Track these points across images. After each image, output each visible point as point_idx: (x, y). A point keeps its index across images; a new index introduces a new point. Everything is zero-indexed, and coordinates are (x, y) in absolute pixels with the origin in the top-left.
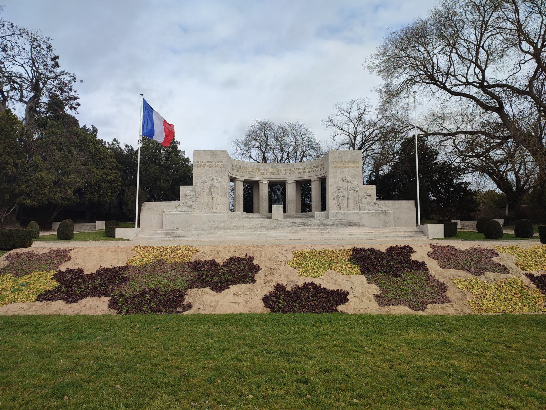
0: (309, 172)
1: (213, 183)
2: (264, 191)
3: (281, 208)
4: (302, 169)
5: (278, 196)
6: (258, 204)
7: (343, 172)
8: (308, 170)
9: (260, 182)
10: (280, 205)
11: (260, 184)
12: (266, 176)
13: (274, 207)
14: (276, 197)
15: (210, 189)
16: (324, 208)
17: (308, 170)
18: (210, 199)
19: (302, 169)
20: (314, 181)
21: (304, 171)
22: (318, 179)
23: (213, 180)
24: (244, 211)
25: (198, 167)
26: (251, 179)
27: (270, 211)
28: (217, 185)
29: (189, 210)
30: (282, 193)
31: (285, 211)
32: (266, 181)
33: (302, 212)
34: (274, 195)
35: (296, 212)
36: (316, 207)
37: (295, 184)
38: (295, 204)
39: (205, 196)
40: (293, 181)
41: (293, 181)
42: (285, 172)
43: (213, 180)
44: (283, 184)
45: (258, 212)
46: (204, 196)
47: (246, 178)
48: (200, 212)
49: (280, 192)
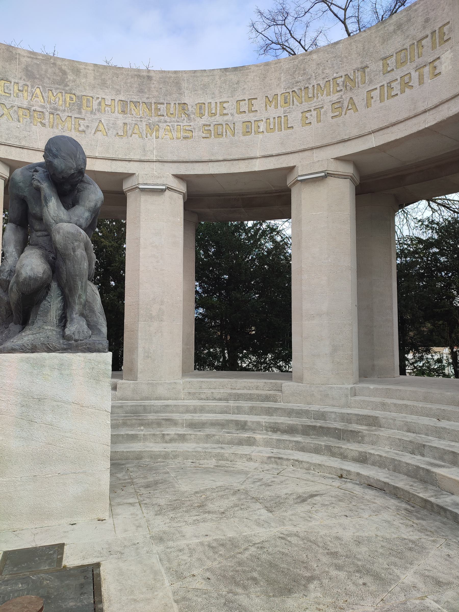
4: (230, 107)
8: (273, 112)
17: (273, 112)
19: (230, 107)
20: (328, 175)
21: (251, 117)
22: (349, 170)
35: (185, 373)
36: (335, 349)
42: (121, 119)
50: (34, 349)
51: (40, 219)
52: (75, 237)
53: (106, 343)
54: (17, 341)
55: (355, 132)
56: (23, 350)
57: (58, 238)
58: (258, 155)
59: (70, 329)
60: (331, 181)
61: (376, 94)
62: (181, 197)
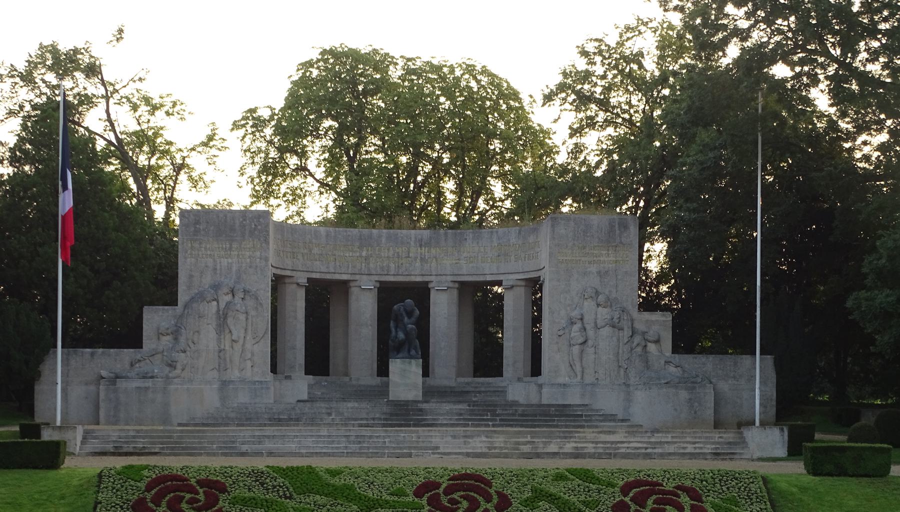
3: (415, 368)
5: (407, 334)
6: (346, 346)
9: (352, 284)
10: (411, 357)
11: (354, 291)
13: (395, 365)
16: (536, 370)
20: (512, 287)
22: (523, 283)
24: (306, 374)
26: (328, 277)
30: (417, 323)
31: (426, 373)
32: (369, 283)
34: (396, 327)
35: (459, 374)
37: (455, 293)
39: (213, 334)
40: (451, 285)
41: (451, 285)
47: (314, 276)
49: (413, 319)
50: (403, 358)
51: (402, 320)
52: (412, 329)
53: (420, 356)
54: (398, 356)
55: (521, 271)
56: (401, 358)
57: (408, 329)
58: (488, 273)
59: (411, 353)
60: (514, 288)
61: (527, 256)
62: (456, 290)
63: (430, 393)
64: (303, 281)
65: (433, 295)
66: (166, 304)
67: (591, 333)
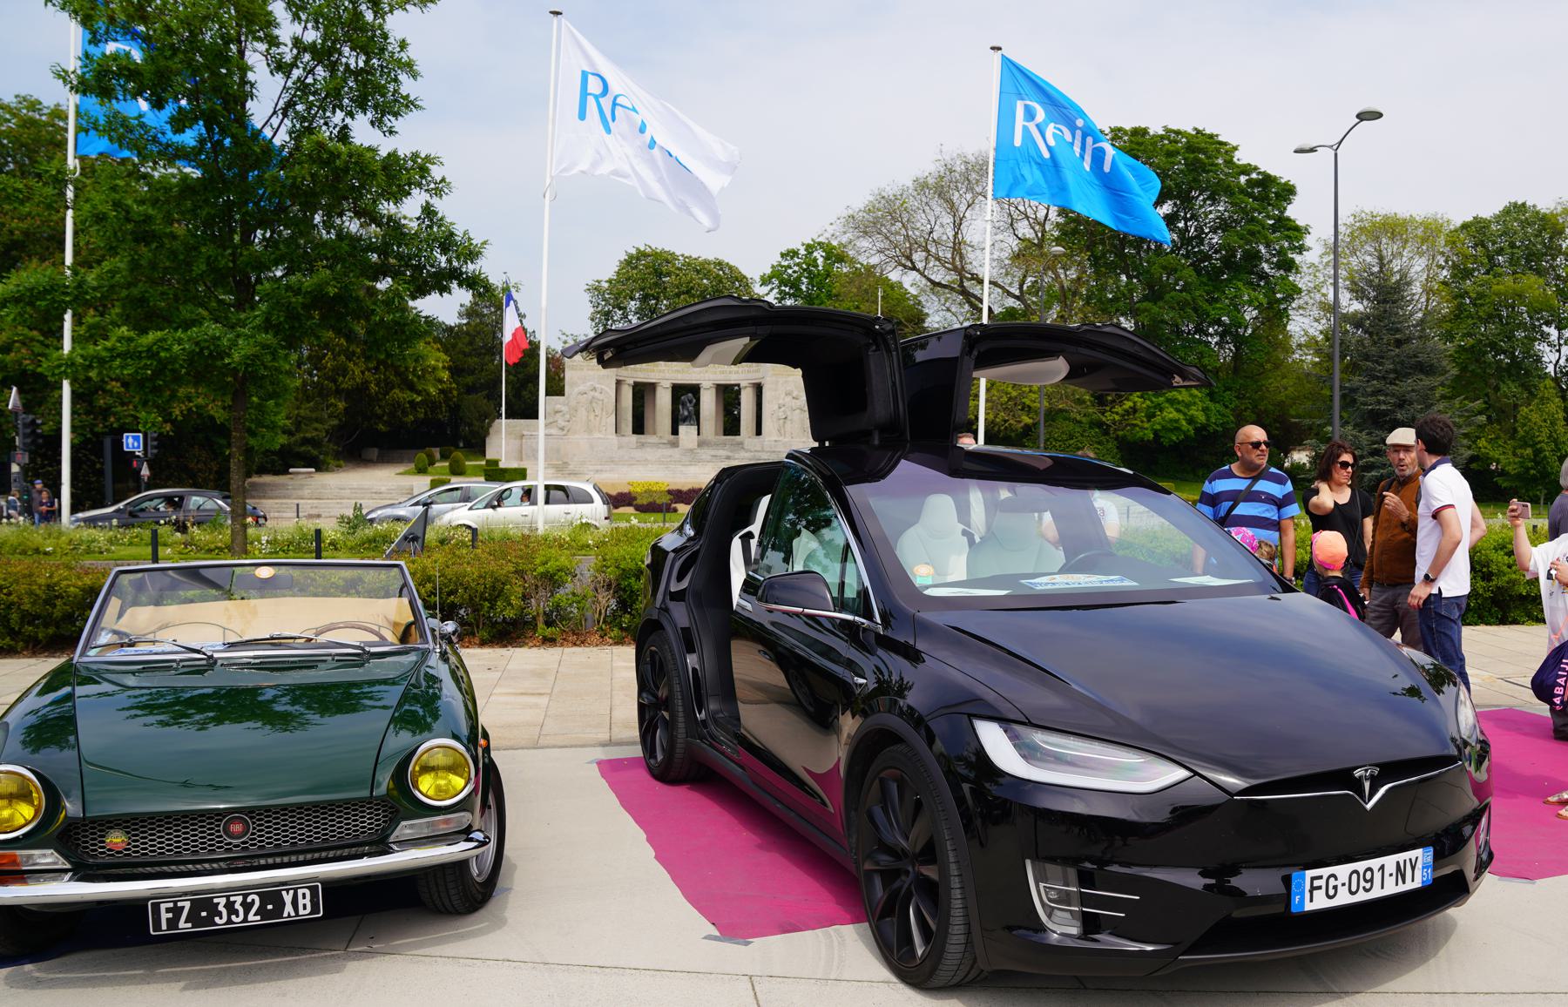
0: (738, 372)
1: (597, 394)
2: (664, 399)
5: (689, 412)
7: (786, 382)
12: (667, 376)
13: (682, 429)
14: (686, 413)
15: (591, 402)
16: (759, 432)
18: (592, 417)
23: (594, 389)
25: (572, 369)
27: (675, 432)
28: (600, 397)
29: (561, 433)
32: (668, 384)
33: (725, 435)
35: (716, 434)
37: (714, 391)
38: (713, 423)
39: (584, 413)
43: (594, 389)
44: (695, 390)
45: (655, 433)
46: (582, 413)
48: (577, 436)
63: (701, 444)
64: (631, 382)
65: (702, 390)
66: (558, 395)
67: (789, 413)
